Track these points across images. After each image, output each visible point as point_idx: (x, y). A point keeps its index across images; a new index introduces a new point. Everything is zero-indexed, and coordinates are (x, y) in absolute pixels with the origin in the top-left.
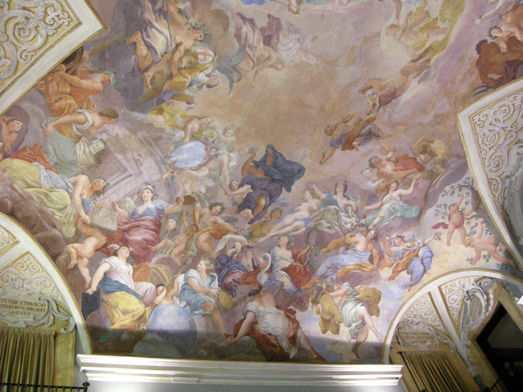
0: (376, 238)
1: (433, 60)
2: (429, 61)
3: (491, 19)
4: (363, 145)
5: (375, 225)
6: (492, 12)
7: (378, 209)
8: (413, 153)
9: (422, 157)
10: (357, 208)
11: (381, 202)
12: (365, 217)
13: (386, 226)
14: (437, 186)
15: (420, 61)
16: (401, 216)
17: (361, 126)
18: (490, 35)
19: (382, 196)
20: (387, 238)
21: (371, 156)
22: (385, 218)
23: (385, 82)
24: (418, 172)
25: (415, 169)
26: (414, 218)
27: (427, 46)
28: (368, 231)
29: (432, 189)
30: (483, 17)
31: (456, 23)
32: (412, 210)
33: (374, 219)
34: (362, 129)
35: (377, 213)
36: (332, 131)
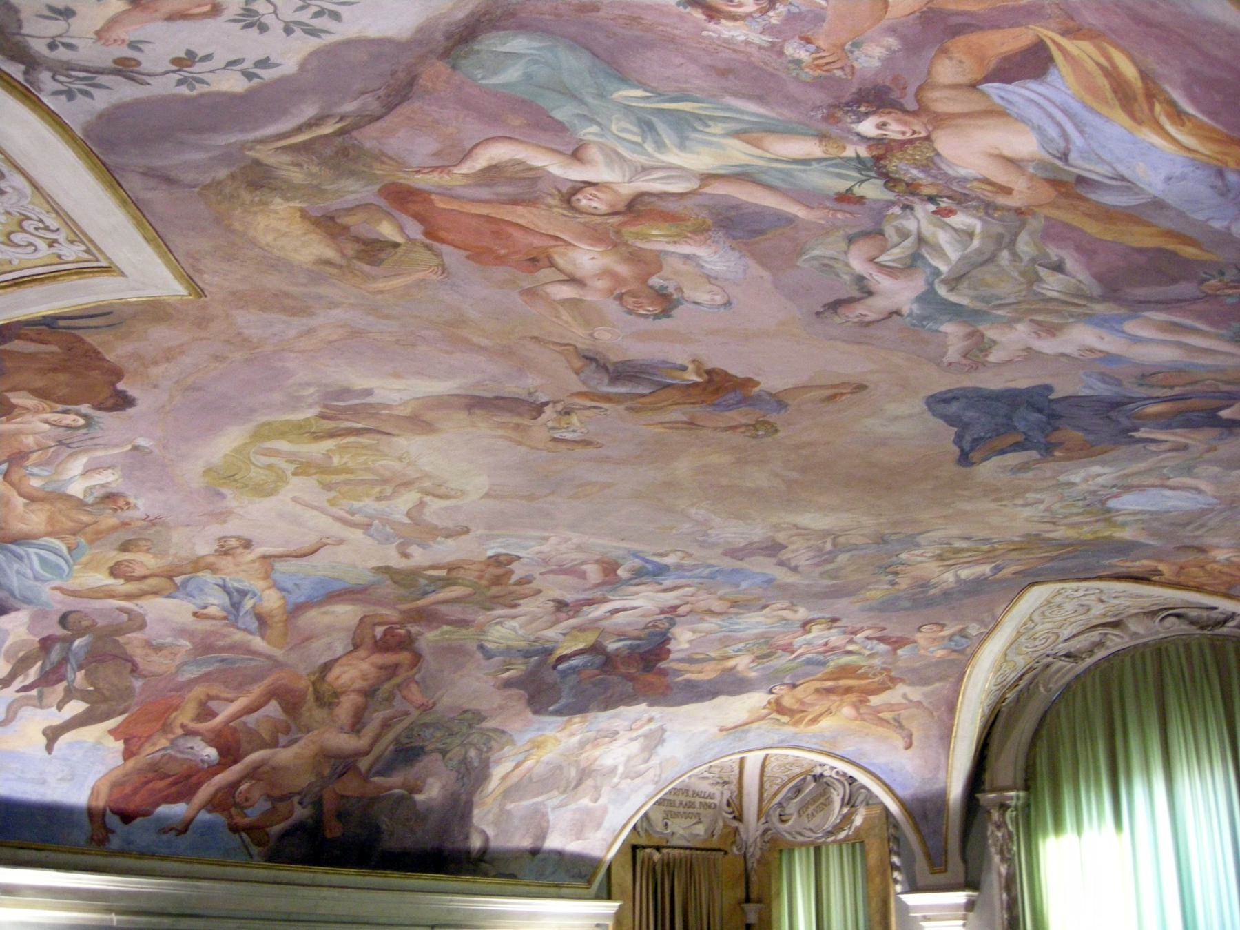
0: (876, 98)
1: (310, 413)
2: (322, 416)
3: (95, 441)
4: (664, 362)
5: (822, 137)
6: (100, 453)
7: (743, 176)
8: (439, 255)
9: (387, 230)
10: (851, 240)
11: (708, 190)
12: (845, 198)
13: (760, 99)
14: (309, 111)
15: (359, 426)
16: (625, 80)
17: (642, 400)
18: (85, 416)
19: (689, 202)
20: (795, 50)
21: (648, 324)
22: (733, 126)
23: (500, 432)
24: (430, 193)
25: (441, 205)
26: (522, 27)
27: (330, 444)
28: (883, 149)
29: (349, 107)
30: (129, 447)
31: (226, 455)
32: (528, 77)
33: (805, 162)
34: (643, 396)
35: (765, 171)
36: (754, 426)
